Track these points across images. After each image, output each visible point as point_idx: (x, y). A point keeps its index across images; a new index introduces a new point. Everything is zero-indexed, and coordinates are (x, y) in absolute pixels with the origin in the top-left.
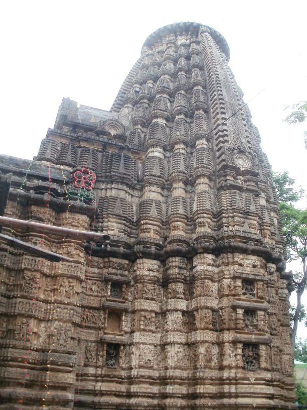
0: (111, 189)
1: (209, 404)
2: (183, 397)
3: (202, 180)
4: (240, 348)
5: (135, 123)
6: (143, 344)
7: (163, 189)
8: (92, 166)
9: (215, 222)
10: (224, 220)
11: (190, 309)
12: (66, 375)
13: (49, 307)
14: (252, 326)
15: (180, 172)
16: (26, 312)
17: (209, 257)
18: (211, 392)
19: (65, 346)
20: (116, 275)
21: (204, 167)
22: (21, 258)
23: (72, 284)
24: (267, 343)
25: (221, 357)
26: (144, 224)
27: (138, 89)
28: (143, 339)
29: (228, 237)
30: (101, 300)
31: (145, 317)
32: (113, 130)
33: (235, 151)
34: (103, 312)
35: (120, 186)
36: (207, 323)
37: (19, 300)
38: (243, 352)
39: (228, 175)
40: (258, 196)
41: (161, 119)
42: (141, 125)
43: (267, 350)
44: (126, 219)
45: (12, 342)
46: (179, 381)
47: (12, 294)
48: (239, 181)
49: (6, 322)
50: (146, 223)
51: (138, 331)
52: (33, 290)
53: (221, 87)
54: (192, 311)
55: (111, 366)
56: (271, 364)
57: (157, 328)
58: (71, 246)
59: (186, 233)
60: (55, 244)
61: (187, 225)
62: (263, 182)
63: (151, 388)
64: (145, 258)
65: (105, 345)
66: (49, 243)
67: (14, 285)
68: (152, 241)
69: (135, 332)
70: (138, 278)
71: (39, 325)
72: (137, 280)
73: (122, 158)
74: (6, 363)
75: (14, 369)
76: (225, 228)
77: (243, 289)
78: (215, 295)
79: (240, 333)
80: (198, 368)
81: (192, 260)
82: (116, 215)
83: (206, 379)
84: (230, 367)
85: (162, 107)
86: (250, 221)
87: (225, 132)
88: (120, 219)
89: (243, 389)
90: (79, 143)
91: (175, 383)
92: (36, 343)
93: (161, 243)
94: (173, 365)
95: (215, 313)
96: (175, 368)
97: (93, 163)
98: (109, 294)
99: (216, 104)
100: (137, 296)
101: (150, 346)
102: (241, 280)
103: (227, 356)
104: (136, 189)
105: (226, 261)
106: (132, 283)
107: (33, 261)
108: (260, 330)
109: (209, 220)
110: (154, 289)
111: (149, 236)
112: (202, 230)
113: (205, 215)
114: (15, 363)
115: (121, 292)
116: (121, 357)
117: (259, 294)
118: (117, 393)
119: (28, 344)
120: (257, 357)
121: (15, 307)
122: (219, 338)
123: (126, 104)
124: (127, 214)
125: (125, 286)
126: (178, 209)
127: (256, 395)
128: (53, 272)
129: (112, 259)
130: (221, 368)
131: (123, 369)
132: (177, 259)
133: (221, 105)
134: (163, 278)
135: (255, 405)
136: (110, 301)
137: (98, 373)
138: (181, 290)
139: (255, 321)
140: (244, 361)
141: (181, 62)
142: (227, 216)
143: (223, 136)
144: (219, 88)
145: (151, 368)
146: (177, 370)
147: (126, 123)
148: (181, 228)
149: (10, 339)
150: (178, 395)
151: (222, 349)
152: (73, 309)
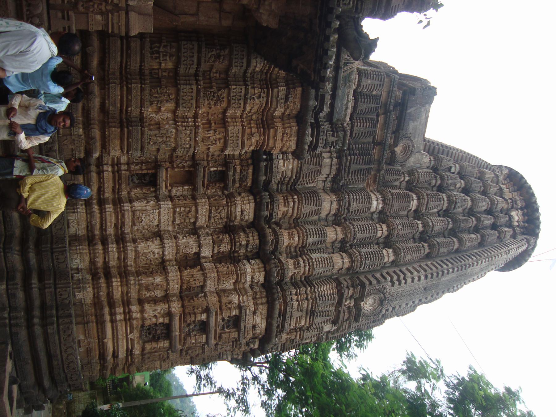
0: (331, 157)
1: (101, 293)
2: (106, 263)
3: (347, 261)
4: (164, 320)
5: (411, 172)
6: (159, 213)
7: (335, 215)
8: (356, 134)
9: (301, 278)
10: (303, 290)
11: (203, 261)
12: (118, 148)
13: (190, 120)
14: (189, 331)
15: (355, 234)
16: (182, 96)
17: (260, 277)
18: (114, 293)
19: (149, 143)
20: (234, 174)
21: (362, 262)
22: (241, 83)
23: (218, 142)
24: (171, 347)
25: (152, 301)
26: (294, 199)
27: (453, 170)
28: (165, 212)
29: (284, 296)
30: (204, 160)
31: (189, 211)
32: (401, 148)
33: (382, 295)
34: (191, 164)
35: (334, 167)
36: (188, 282)
37: (194, 87)
38: (160, 324)
39: (354, 290)
40: (334, 322)
41: (417, 204)
42: (407, 182)
43: (164, 348)
44: (297, 178)
45: (147, 87)
46: (122, 257)
47: (200, 78)
48: (348, 302)
49: (169, 76)
50: (294, 202)
51: (173, 205)
52: (207, 102)
53: (458, 271)
54: (201, 264)
55: (130, 179)
56: (149, 353)
57: (178, 225)
58: (260, 136)
59: (287, 247)
60: (260, 117)
61: (296, 247)
62: (349, 327)
63: (111, 226)
64: (255, 205)
65: (153, 171)
66: (261, 110)
67: (210, 79)
68: (275, 210)
69: (172, 201)
70: (233, 199)
71: (168, 111)
72: (230, 197)
73: (367, 167)
74: (125, 83)
75: (119, 93)
76: (294, 292)
77: (229, 317)
78: (220, 287)
79: (180, 319)
80: (138, 276)
81: (256, 258)
82: (301, 168)
83: (128, 288)
84: (142, 311)
85: (431, 204)
86: (304, 317)
87: (403, 281)
88: (297, 171)
89: (121, 328)
90: (383, 114)
91: (119, 252)
92: (149, 112)
93: (273, 220)
94: (139, 249)
95: (200, 289)
96: (136, 251)
97: (359, 134)
98: (212, 169)
99: (437, 268)
100: (212, 200)
101: (157, 220)
102: (238, 314)
103: (154, 308)
104: (332, 185)
105: (258, 296)
106: (226, 192)
107: (239, 98)
108: (185, 339)
109: (302, 272)
110: (221, 218)
111: (280, 206)
112: (290, 267)
113: (307, 268)
114: (125, 92)
115: (215, 182)
116: (142, 189)
117: (224, 335)
118: (102, 189)
119: (147, 103)
120: (156, 339)
121: (186, 85)
122: (173, 296)
123: (435, 158)
124: (303, 178)
125: (222, 185)
126: (312, 236)
127: (115, 341)
128: (229, 120)
129: (251, 168)
130: (141, 302)
131: (129, 193)
132: (257, 242)
133: (435, 274)
134: (234, 226)
135: (105, 341)
136: (204, 171)
137: (122, 166)
138: (222, 249)
139: (195, 333)
140: (150, 325)
141: (488, 220)
142: (308, 292)
143: (399, 280)
144: (456, 269)
145: (134, 224)
146: (133, 253)
147: (412, 162)
148: (292, 241)
149: (150, 82)
150: (107, 257)
151: (161, 301)
152: (190, 147)
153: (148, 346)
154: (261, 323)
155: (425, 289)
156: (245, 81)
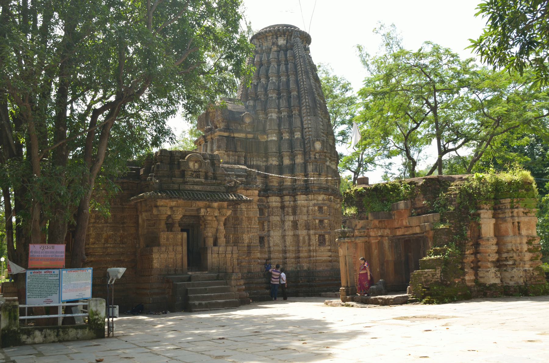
11: (295, 220)
132: (288, 197)
153: (327, 244)
154: (321, 197)
155: (314, 116)
156: (236, 211)
